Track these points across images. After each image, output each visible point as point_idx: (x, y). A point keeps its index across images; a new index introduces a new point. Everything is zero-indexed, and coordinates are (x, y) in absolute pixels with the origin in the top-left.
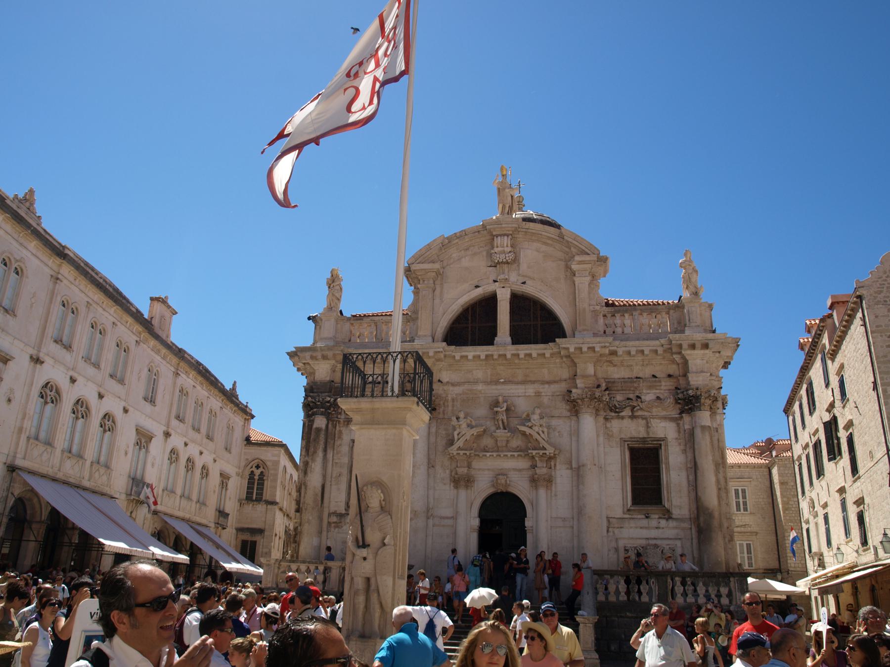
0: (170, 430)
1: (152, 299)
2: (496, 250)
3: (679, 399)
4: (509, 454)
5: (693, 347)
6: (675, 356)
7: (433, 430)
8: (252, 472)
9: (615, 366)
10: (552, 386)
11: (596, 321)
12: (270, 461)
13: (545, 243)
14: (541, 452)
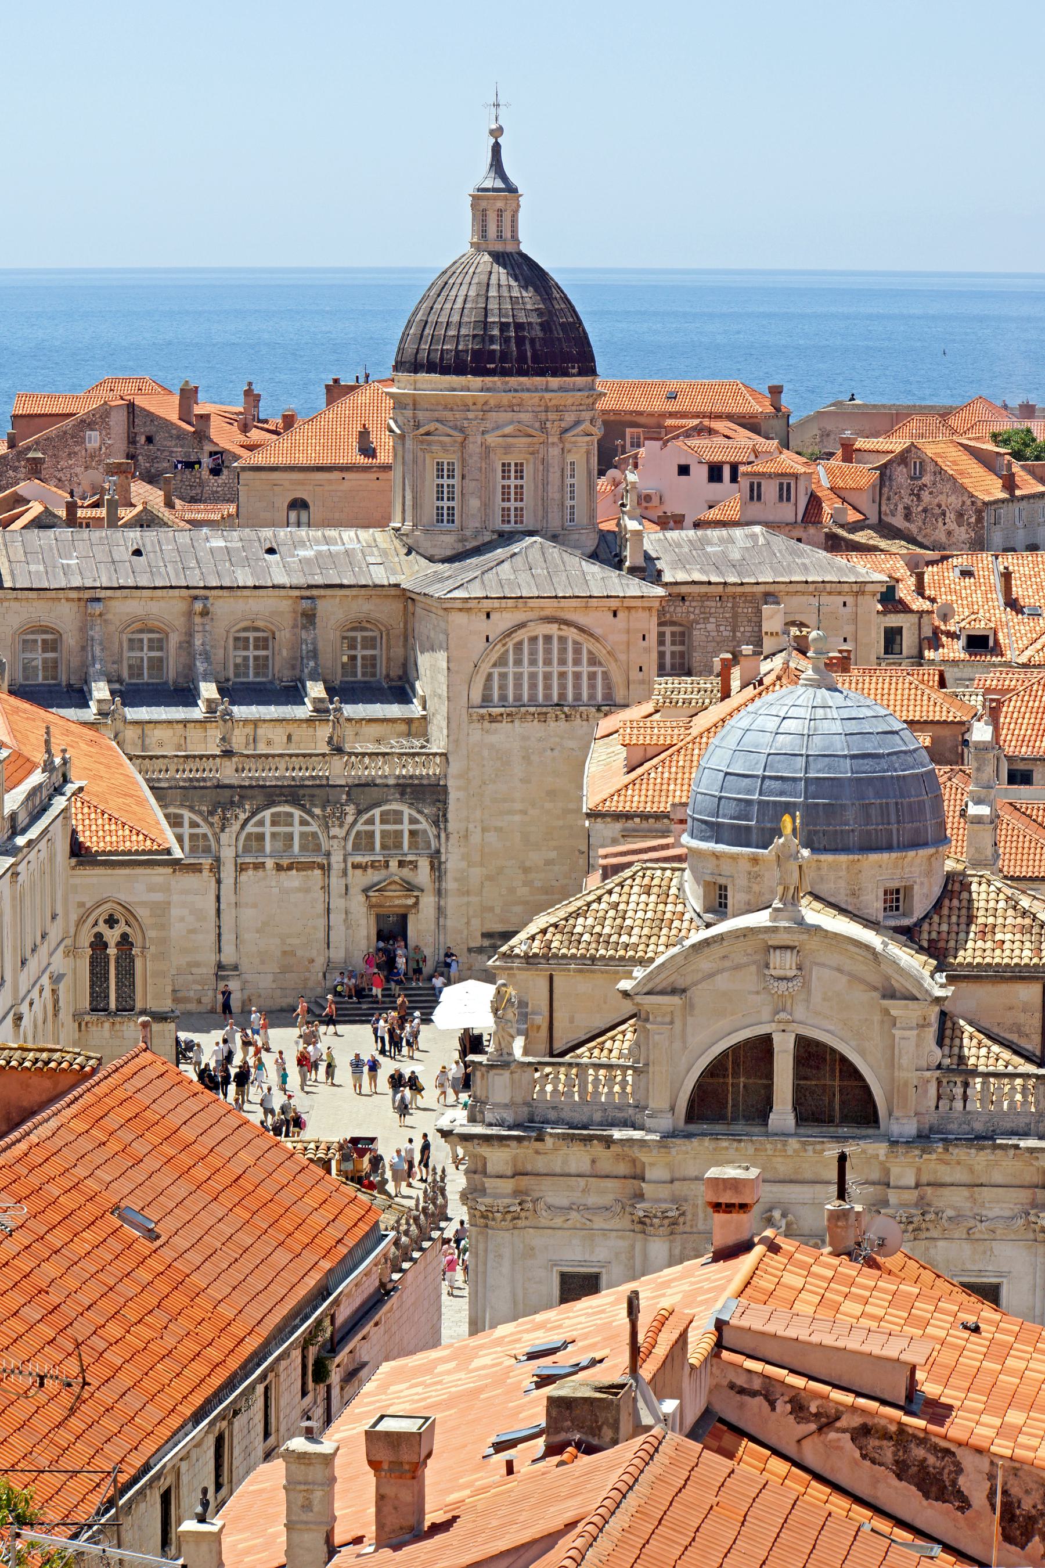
8: (99, 936)
12: (143, 904)
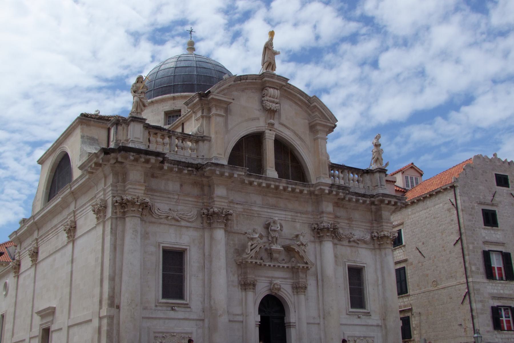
3: (375, 236)
9: (338, 206)
14: (305, 266)
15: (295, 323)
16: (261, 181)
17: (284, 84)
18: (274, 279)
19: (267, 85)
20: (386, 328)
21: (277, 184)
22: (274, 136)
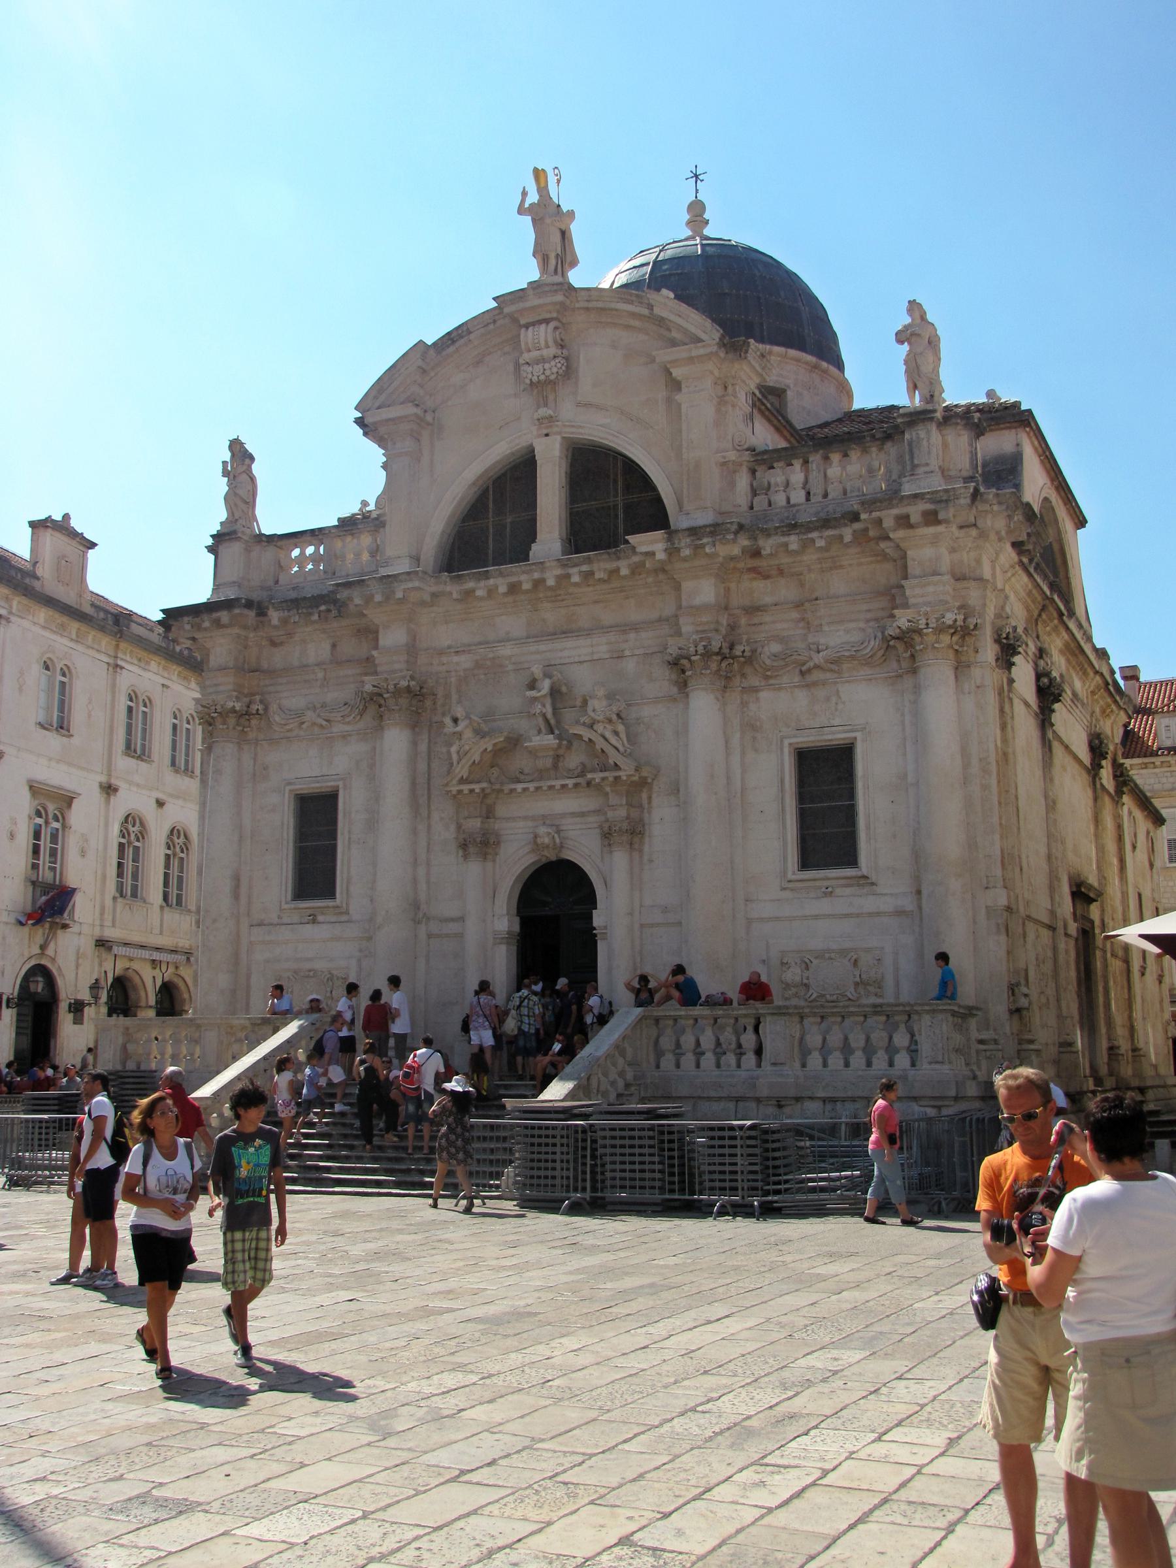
0: (113, 781)
1: (33, 525)
2: (527, 356)
4: (558, 783)
5: (904, 521)
6: (883, 545)
7: (423, 747)
9: (767, 577)
10: (644, 635)
11: (732, 484)
13: (628, 327)
14: (610, 775)
15: (605, 928)
16: (492, 581)
17: (559, 298)
18: (552, 818)
19: (523, 322)
20: (921, 919)
21: (536, 575)
22: (557, 446)
